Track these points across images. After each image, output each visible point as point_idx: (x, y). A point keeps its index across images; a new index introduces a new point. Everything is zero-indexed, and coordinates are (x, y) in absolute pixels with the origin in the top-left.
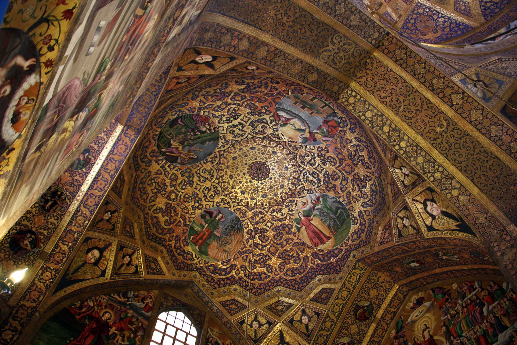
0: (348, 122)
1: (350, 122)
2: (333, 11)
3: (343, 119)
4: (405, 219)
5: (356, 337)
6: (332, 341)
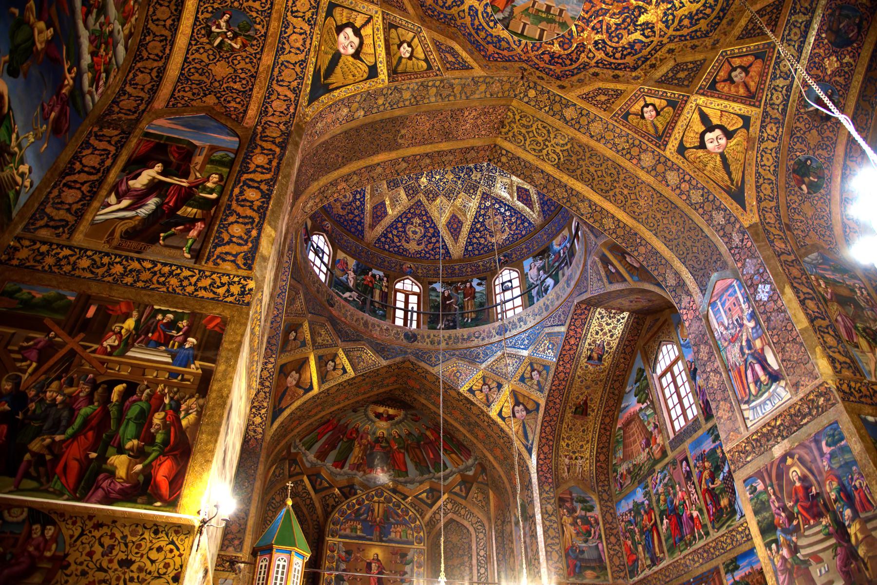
0: (484, 24)
1: (483, 28)
2: (569, 192)
3: (492, 24)
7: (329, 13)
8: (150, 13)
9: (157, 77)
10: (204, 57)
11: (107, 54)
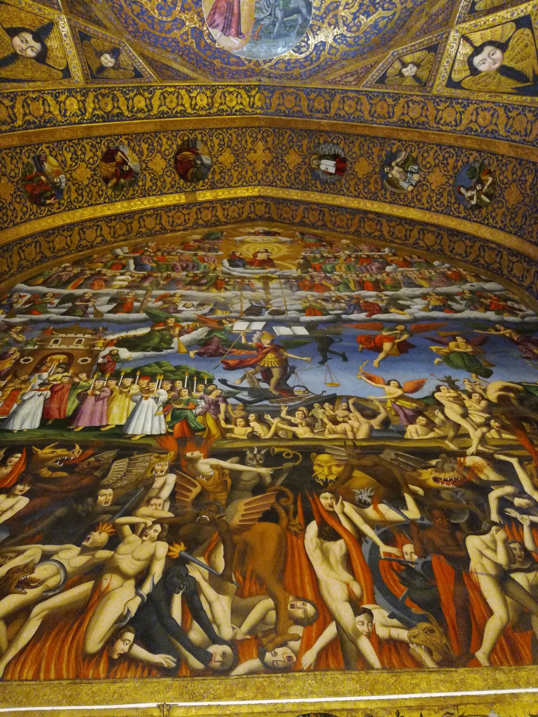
4: (410, 66)
5: (149, 178)
6: (118, 131)
7: (457, 85)
8: (460, 258)
9: (517, 257)
10: (500, 212)
11: (490, 298)
